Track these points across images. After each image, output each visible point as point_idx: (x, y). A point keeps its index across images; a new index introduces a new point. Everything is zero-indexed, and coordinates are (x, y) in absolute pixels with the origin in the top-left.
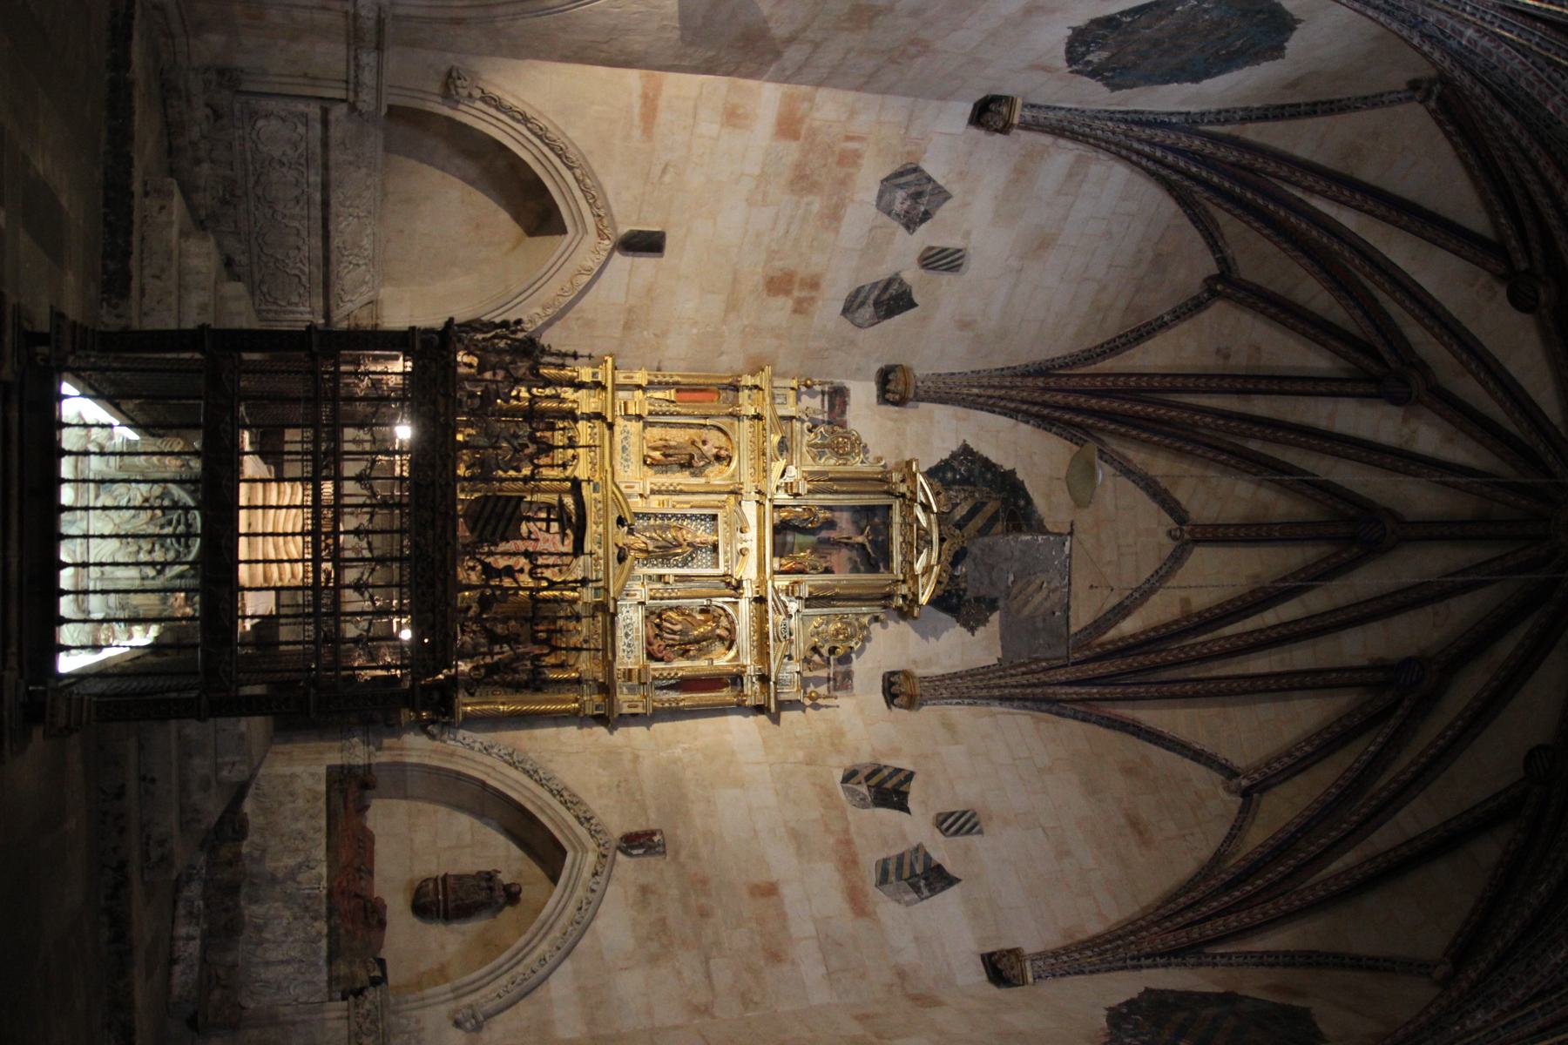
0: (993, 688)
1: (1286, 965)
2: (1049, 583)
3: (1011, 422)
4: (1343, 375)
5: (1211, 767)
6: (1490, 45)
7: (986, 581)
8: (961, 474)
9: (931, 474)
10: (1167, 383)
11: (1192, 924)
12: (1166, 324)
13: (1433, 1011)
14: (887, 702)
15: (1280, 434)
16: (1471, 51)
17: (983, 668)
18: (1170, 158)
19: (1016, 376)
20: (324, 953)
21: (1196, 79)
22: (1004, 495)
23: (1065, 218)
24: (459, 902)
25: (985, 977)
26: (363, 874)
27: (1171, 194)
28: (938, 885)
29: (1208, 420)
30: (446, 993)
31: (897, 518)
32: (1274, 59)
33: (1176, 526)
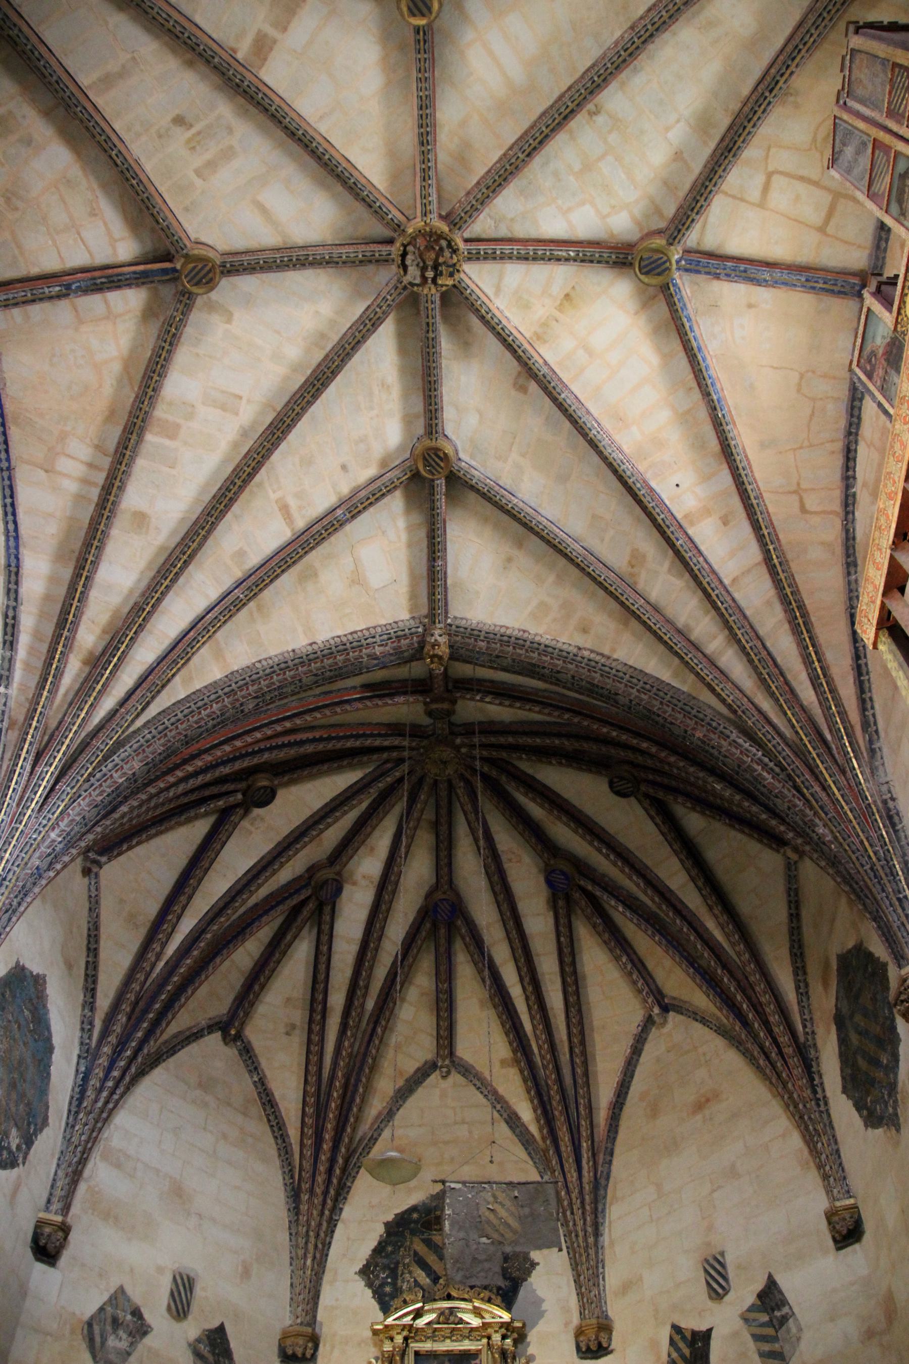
0: (587, 1242)
1: (805, 973)
2: (488, 1203)
3: (340, 1226)
4: (315, 931)
5: (646, 1039)
6: (66, 821)
7: (487, 1265)
8: (387, 1277)
9: (386, 1309)
10: (312, 1079)
11: (780, 1053)
12: (260, 1079)
13: (823, 864)
14: (606, 1355)
15: (361, 983)
16: (68, 834)
18: (116, 1073)
19: (297, 1220)
21: (50, 1049)
22: (407, 1234)
23: (157, 1171)
25: (857, 1246)
27: (147, 1073)
28: (778, 1297)
29: (346, 1044)
31: (427, 1346)
32: (45, 982)
33: (438, 1072)
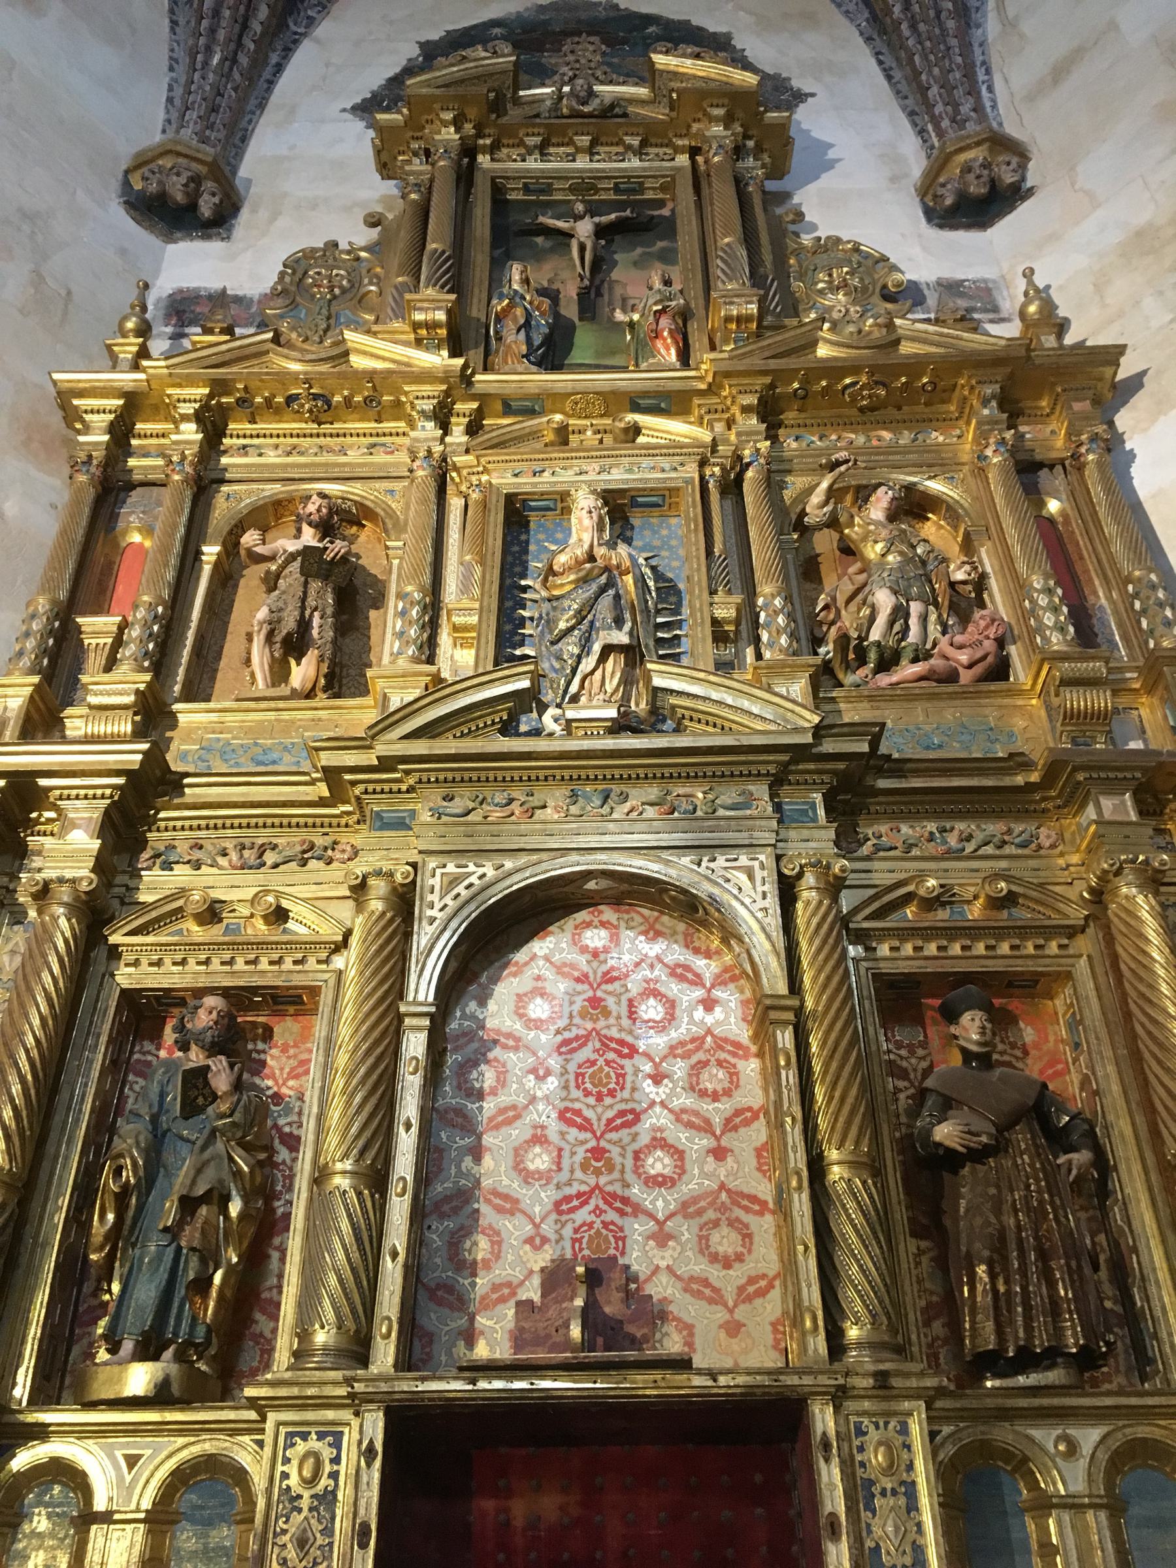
17: (889, 78)
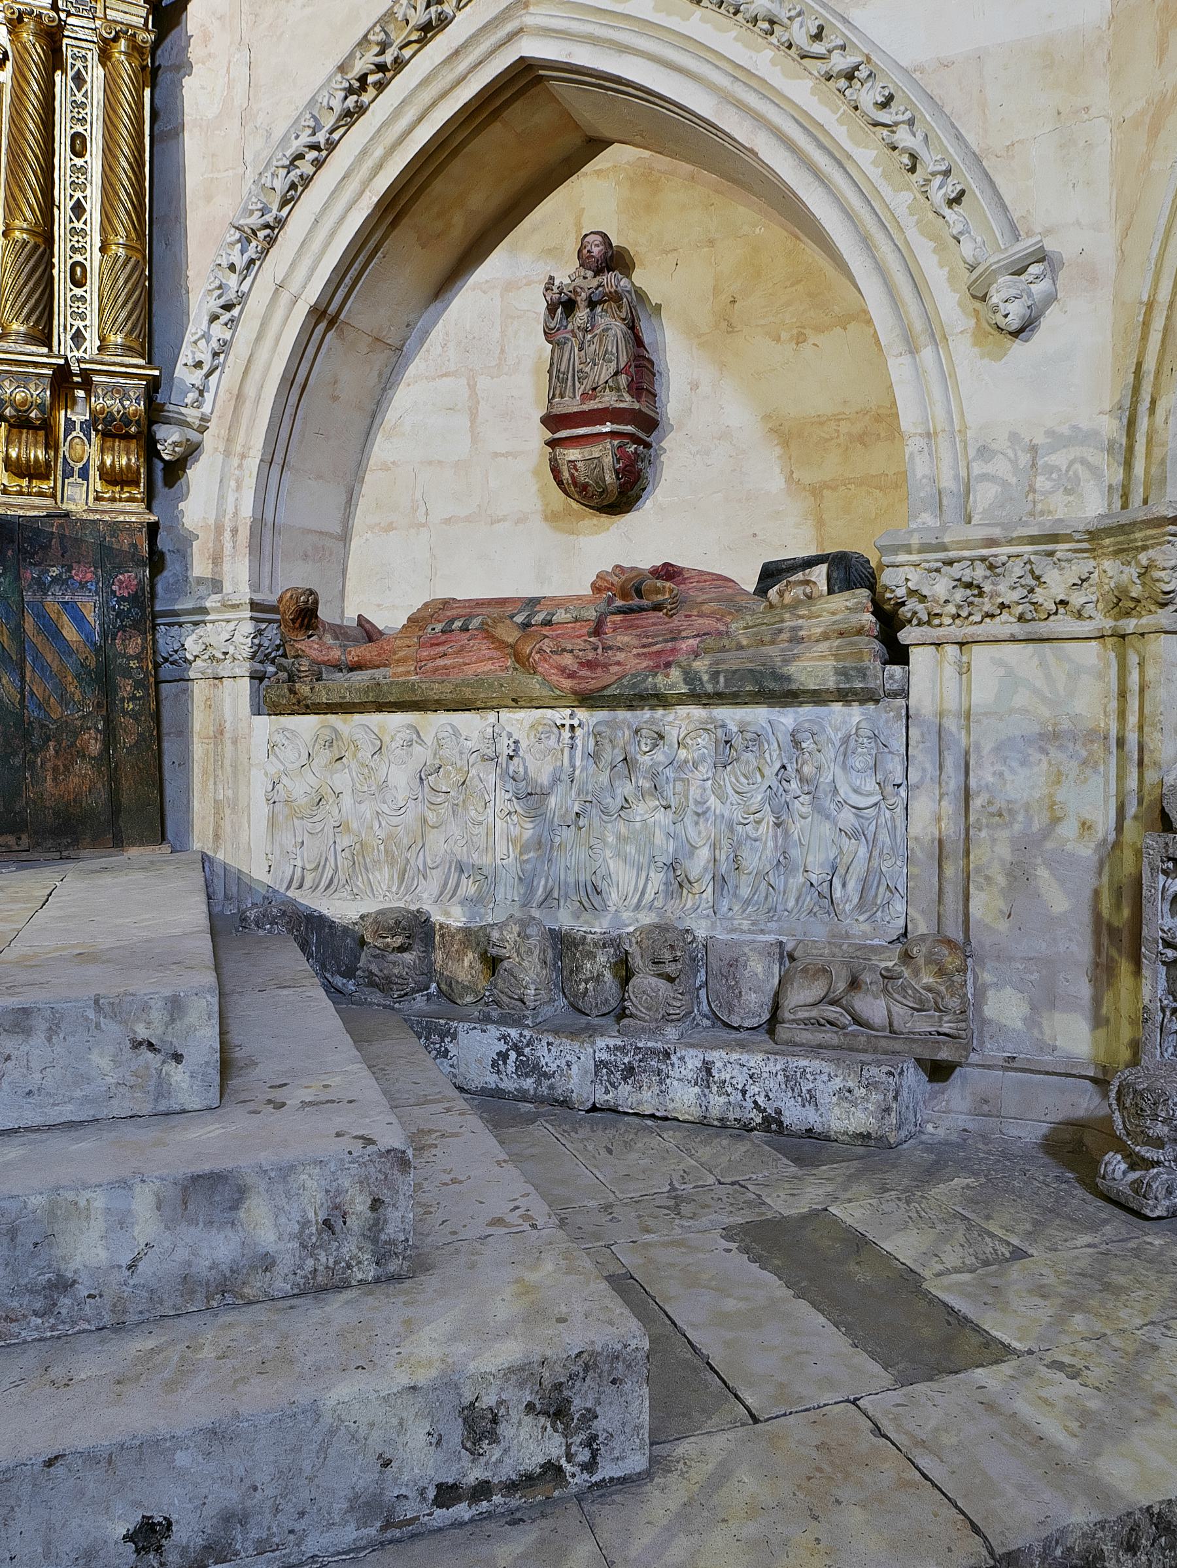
20: (759, 715)
24: (623, 379)
26: (539, 618)
30: (919, 373)
